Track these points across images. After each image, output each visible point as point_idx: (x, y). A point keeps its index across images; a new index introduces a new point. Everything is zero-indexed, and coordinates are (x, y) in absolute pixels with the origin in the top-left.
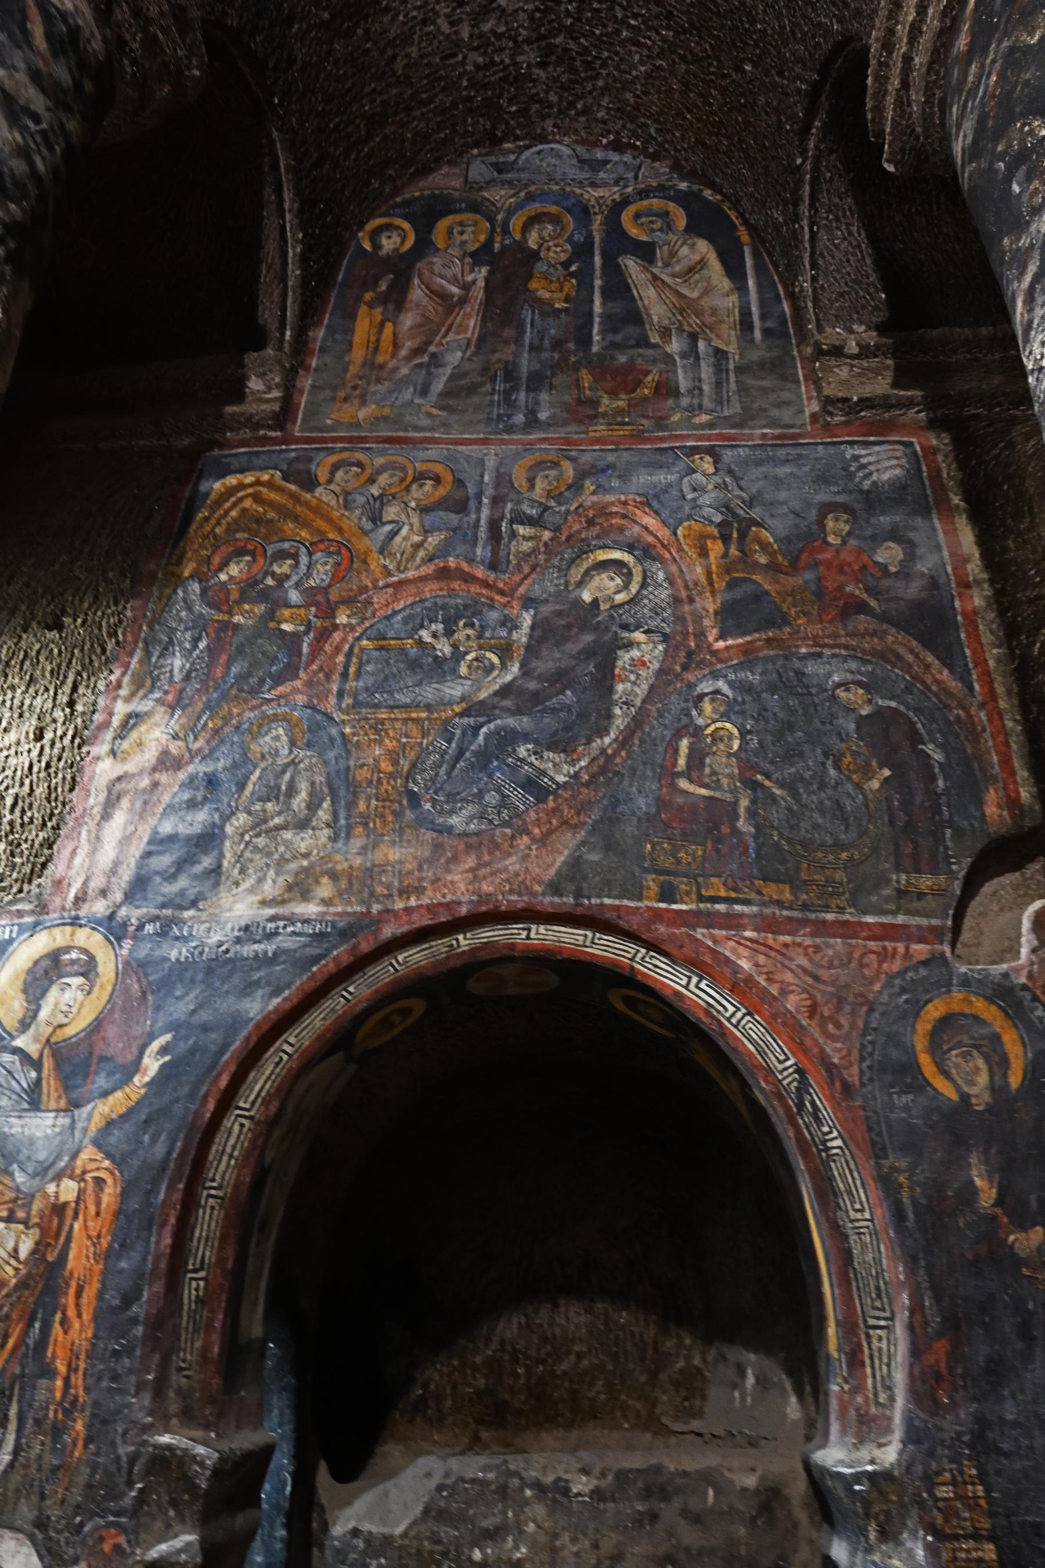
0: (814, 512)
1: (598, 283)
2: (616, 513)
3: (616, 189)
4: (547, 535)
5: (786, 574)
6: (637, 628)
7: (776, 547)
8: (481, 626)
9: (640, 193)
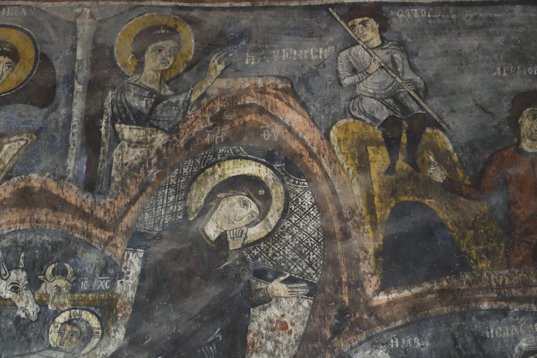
0: (506, 104)
2: (251, 105)
4: (160, 139)
5: (468, 197)
6: (277, 275)
7: (455, 157)
8: (75, 274)
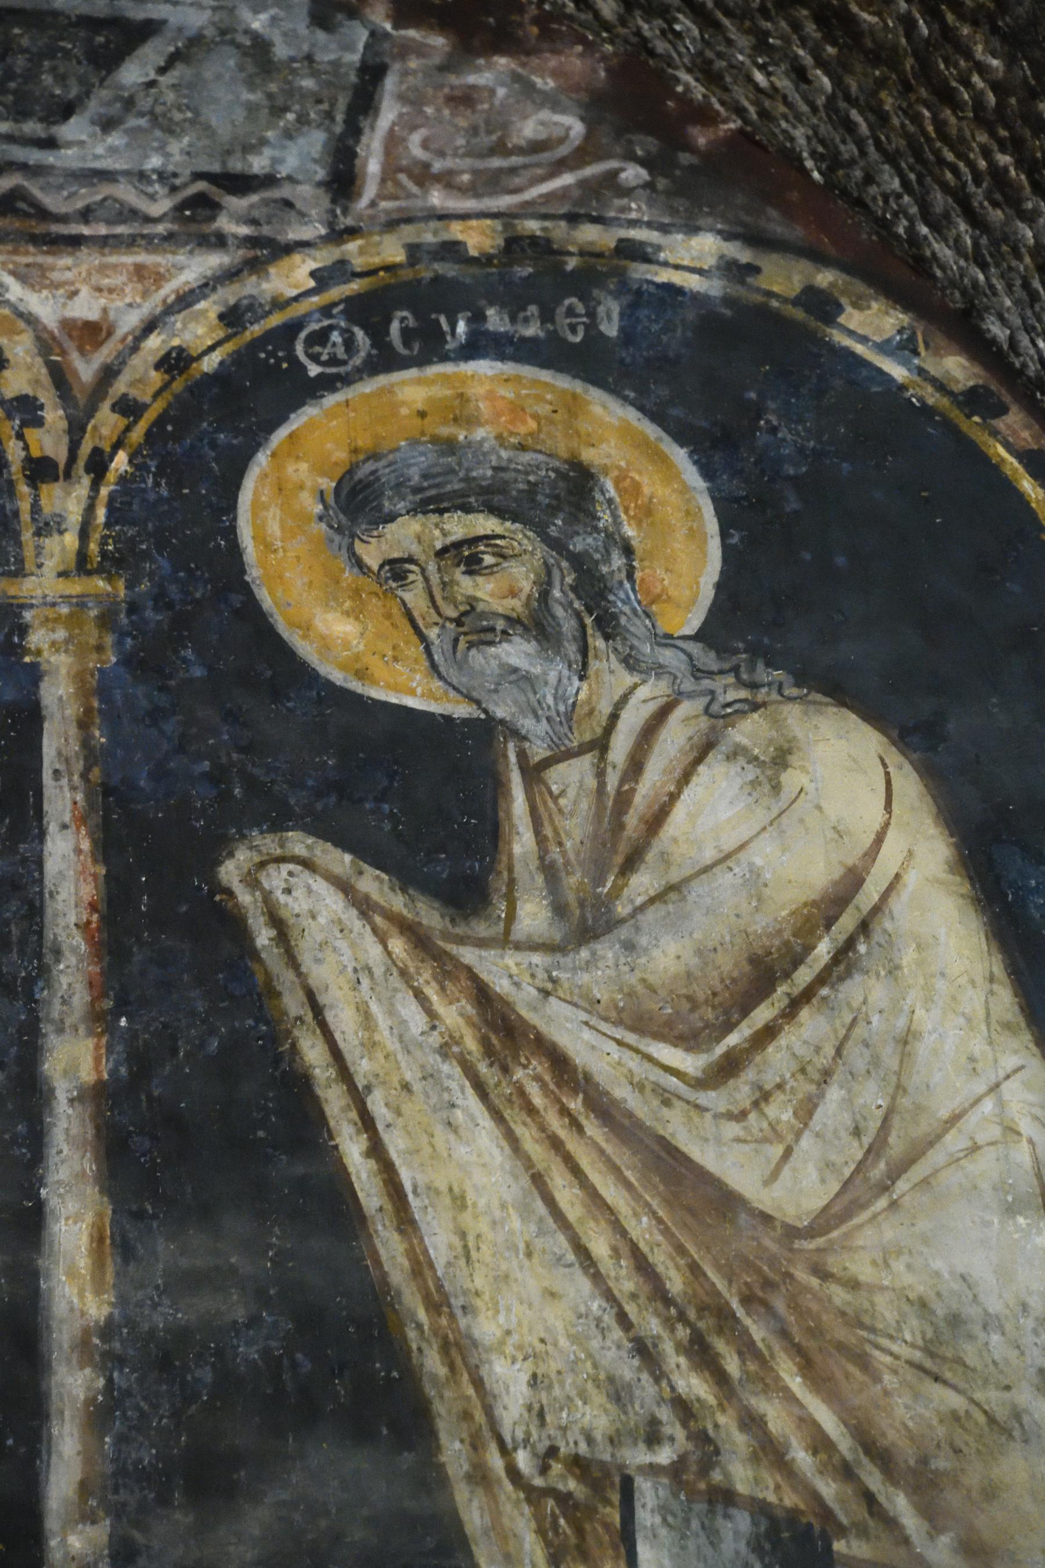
1: (73, 1060)
3: (195, 267)
9: (368, 310)
